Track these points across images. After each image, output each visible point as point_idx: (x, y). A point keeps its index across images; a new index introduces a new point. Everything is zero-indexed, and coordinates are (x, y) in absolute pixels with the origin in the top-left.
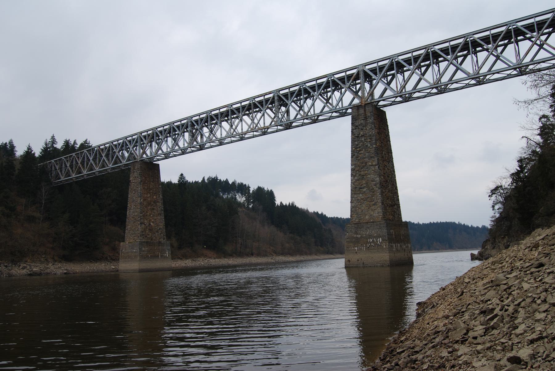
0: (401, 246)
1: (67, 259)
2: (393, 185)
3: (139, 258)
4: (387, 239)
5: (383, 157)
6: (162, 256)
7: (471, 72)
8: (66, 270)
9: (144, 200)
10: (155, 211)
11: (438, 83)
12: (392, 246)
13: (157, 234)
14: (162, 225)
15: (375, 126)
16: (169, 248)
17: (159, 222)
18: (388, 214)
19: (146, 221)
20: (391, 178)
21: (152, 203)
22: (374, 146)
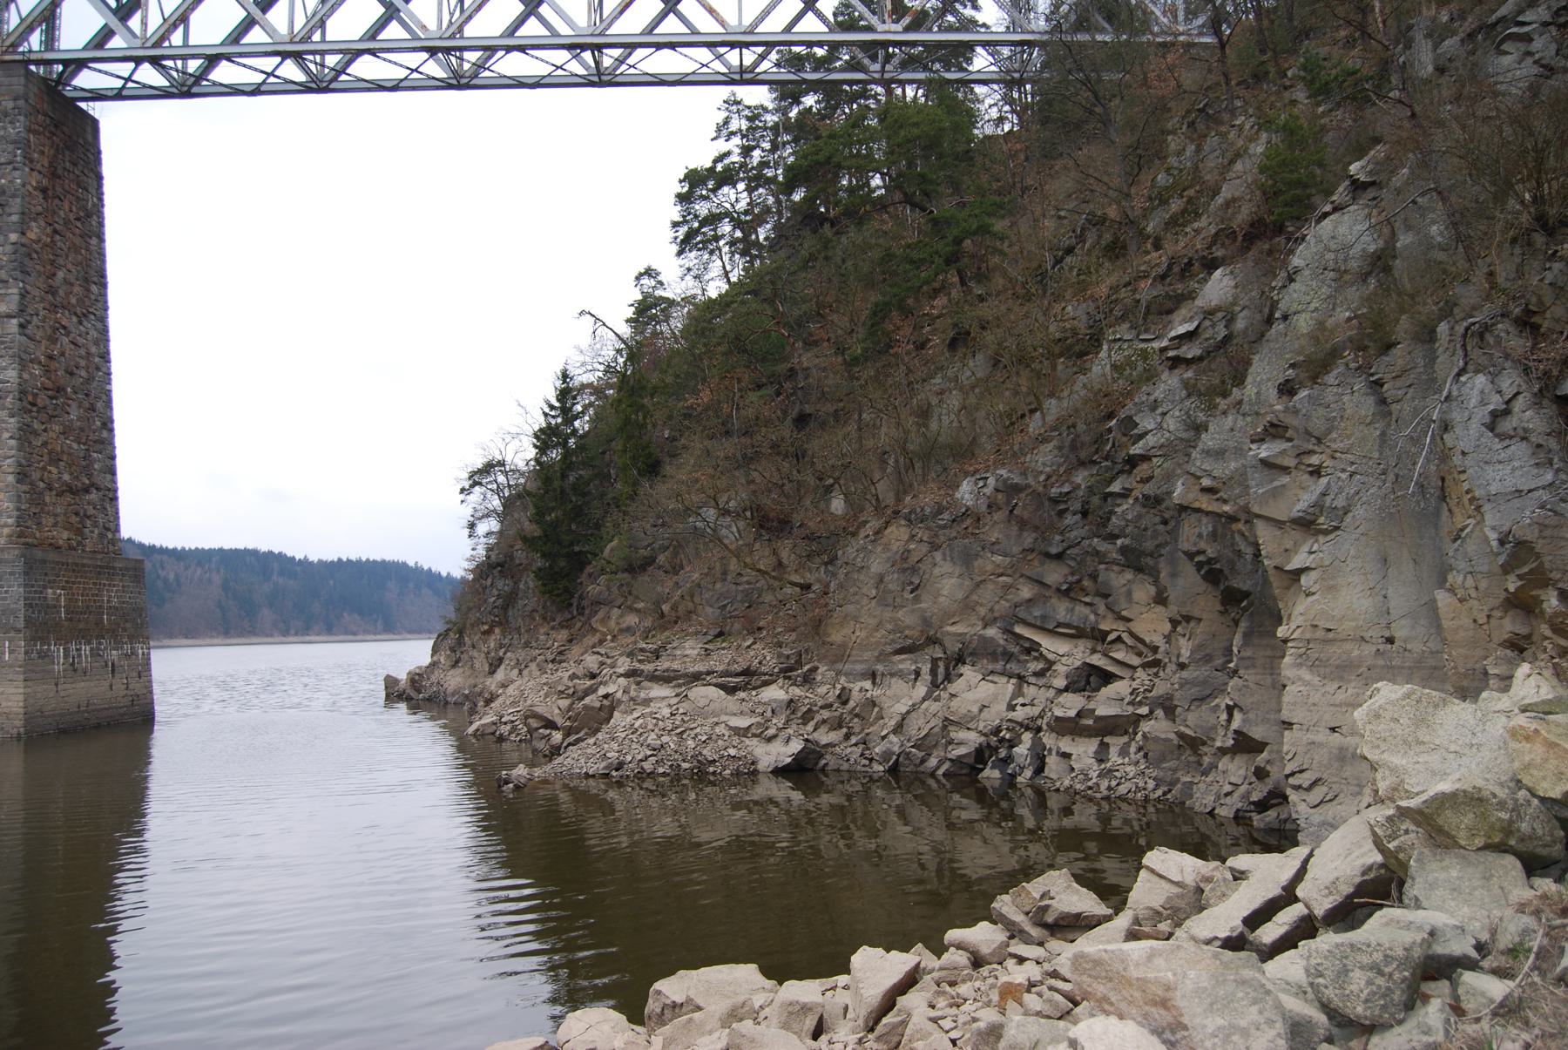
0: (95, 653)
2: (92, 408)
4: (21, 624)
5: (52, 291)
7: (432, 25)
11: (307, 39)
12: (43, 655)
15: (28, 159)
18: (48, 521)
20: (89, 380)
22: (13, 237)
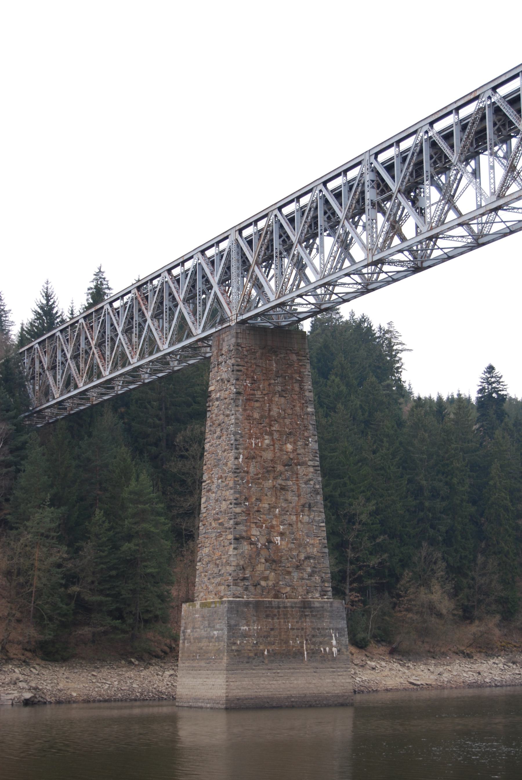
1: (51, 652)
3: (225, 660)
6: (313, 653)
8: (36, 689)
9: (249, 458)
10: (290, 496)
13: (295, 575)
14: (316, 543)
16: (343, 624)
17: (306, 533)
19: (255, 531)
21: (280, 468)
